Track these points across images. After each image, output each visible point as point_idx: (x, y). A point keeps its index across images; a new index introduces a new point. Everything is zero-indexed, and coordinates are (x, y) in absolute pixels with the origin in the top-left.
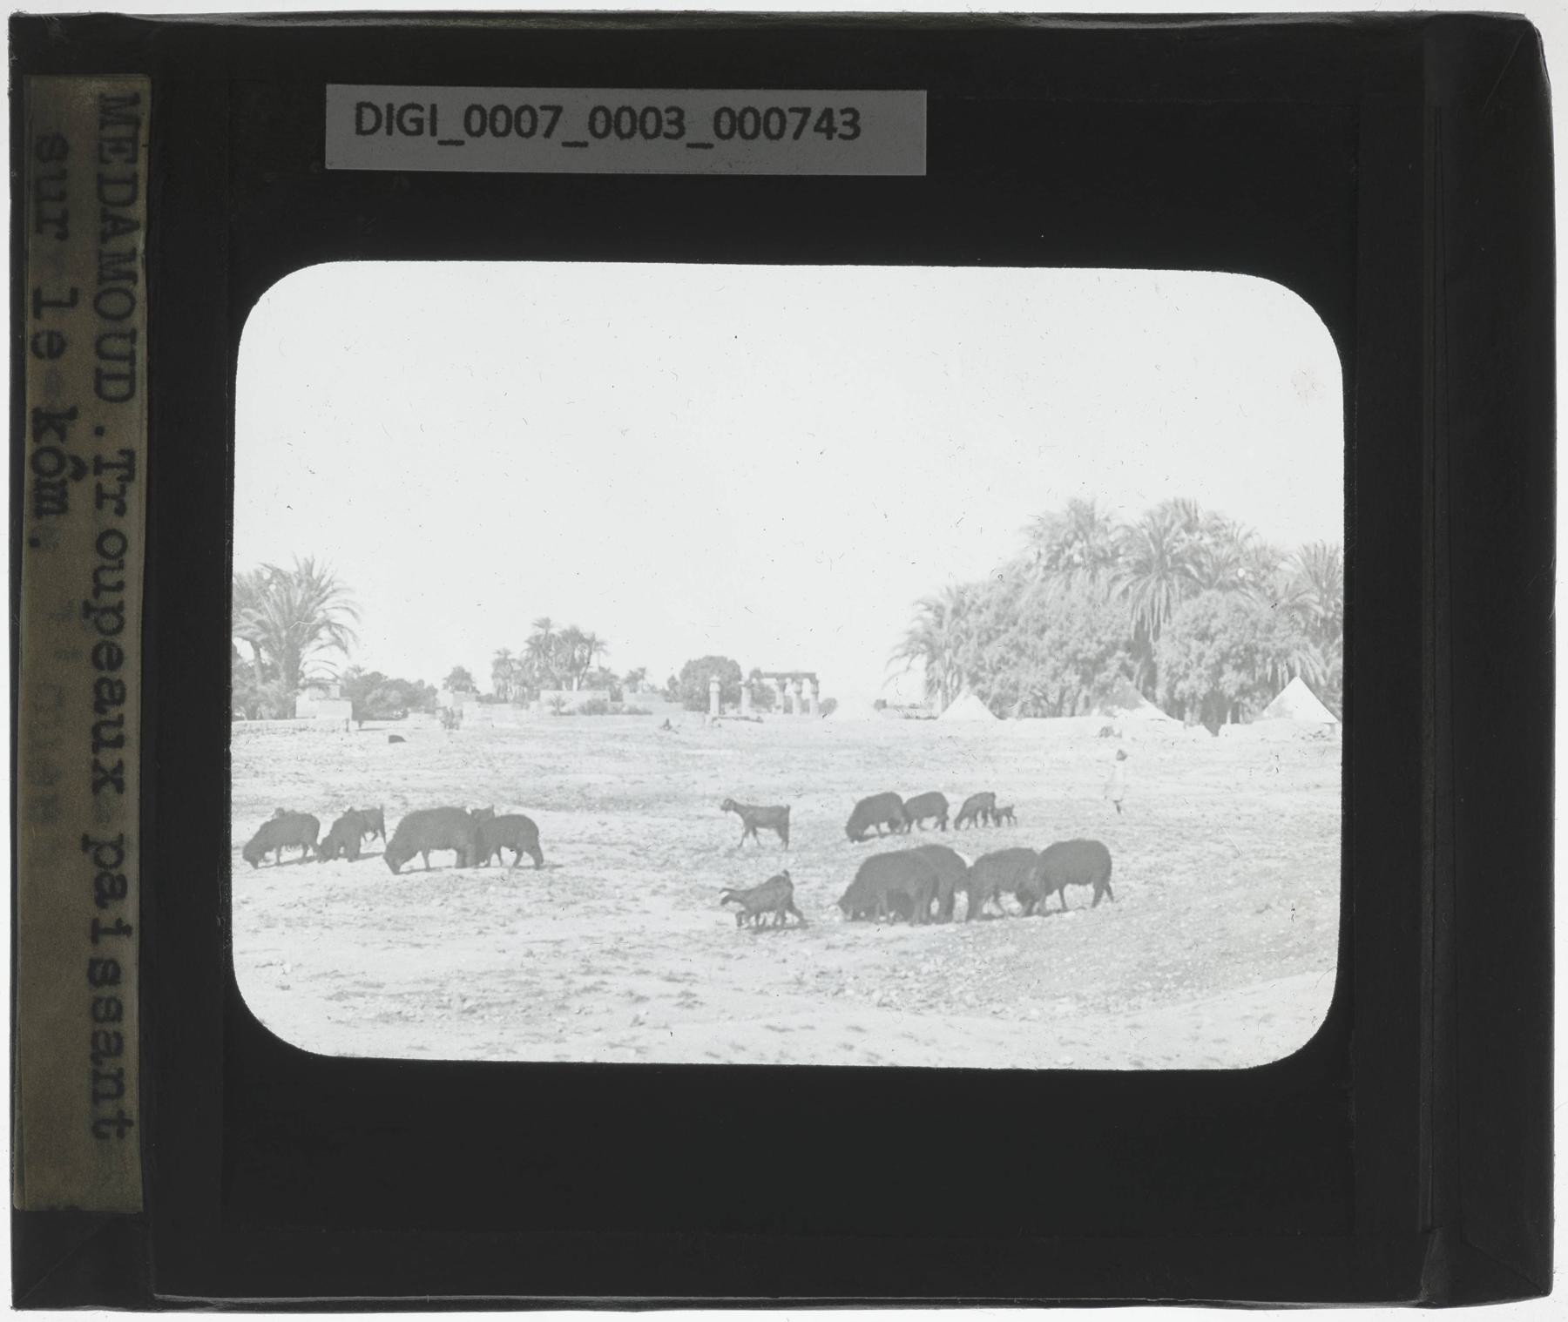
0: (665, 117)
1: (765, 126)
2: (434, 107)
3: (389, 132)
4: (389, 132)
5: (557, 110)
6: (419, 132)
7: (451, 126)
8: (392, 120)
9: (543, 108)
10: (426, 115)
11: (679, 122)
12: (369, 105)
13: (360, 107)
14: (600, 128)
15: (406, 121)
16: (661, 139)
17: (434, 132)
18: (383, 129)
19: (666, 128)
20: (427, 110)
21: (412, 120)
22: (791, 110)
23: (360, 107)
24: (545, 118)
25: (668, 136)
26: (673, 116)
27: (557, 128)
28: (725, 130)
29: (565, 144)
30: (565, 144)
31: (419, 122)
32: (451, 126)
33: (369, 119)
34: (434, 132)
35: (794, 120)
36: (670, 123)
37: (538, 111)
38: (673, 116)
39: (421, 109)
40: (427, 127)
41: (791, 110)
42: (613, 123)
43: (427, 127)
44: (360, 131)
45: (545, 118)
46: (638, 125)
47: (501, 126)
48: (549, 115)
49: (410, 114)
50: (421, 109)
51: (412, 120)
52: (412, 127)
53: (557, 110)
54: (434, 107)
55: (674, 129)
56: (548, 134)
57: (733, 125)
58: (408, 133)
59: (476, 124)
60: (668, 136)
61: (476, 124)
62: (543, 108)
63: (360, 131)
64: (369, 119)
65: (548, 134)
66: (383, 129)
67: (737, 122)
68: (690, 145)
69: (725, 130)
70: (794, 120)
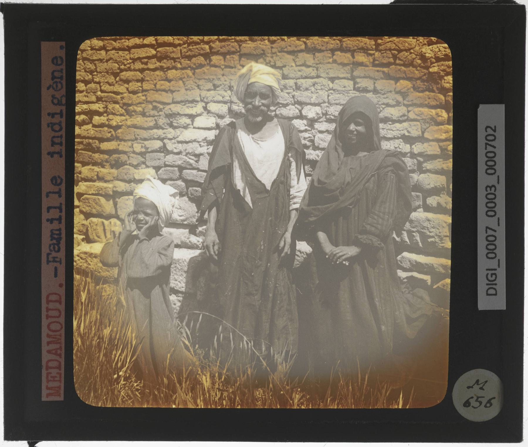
0: (489, 192)
1: (491, 158)
2: (487, 270)
3: (496, 284)
4: (496, 284)
5: (487, 228)
6: (495, 274)
7: (493, 264)
8: (491, 284)
9: (486, 233)
10: (490, 272)
11: (491, 187)
12: (487, 291)
13: (488, 294)
14: (493, 213)
15: (490, 278)
16: (496, 193)
17: (495, 270)
18: (494, 286)
19: (493, 191)
20: (488, 272)
21: (492, 277)
22: (486, 149)
23: (488, 294)
24: (490, 232)
25: (495, 191)
26: (488, 189)
27: (493, 228)
28: (493, 171)
29: (499, 225)
30: (499, 225)
31: (492, 274)
32: (493, 264)
33: (492, 291)
34: (495, 270)
35: (490, 149)
36: (491, 190)
37: (487, 234)
38: (488, 189)
39: (488, 274)
40: (493, 272)
41: (486, 149)
42: (491, 209)
43: (493, 272)
44: (496, 294)
45: (490, 232)
46: (491, 200)
47: (493, 247)
48: (488, 230)
49: (489, 276)
50: (488, 274)
51: (492, 277)
52: (494, 276)
53: (487, 228)
54: (487, 270)
55: (493, 189)
56: (495, 231)
57: (491, 168)
58: (496, 277)
59: (492, 255)
60: (495, 191)
61: (492, 255)
62: (486, 233)
63: (496, 294)
64: (492, 291)
65: (495, 231)
66: (494, 286)
67: (491, 167)
68: (498, 183)
69: (493, 171)
70: (490, 149)
